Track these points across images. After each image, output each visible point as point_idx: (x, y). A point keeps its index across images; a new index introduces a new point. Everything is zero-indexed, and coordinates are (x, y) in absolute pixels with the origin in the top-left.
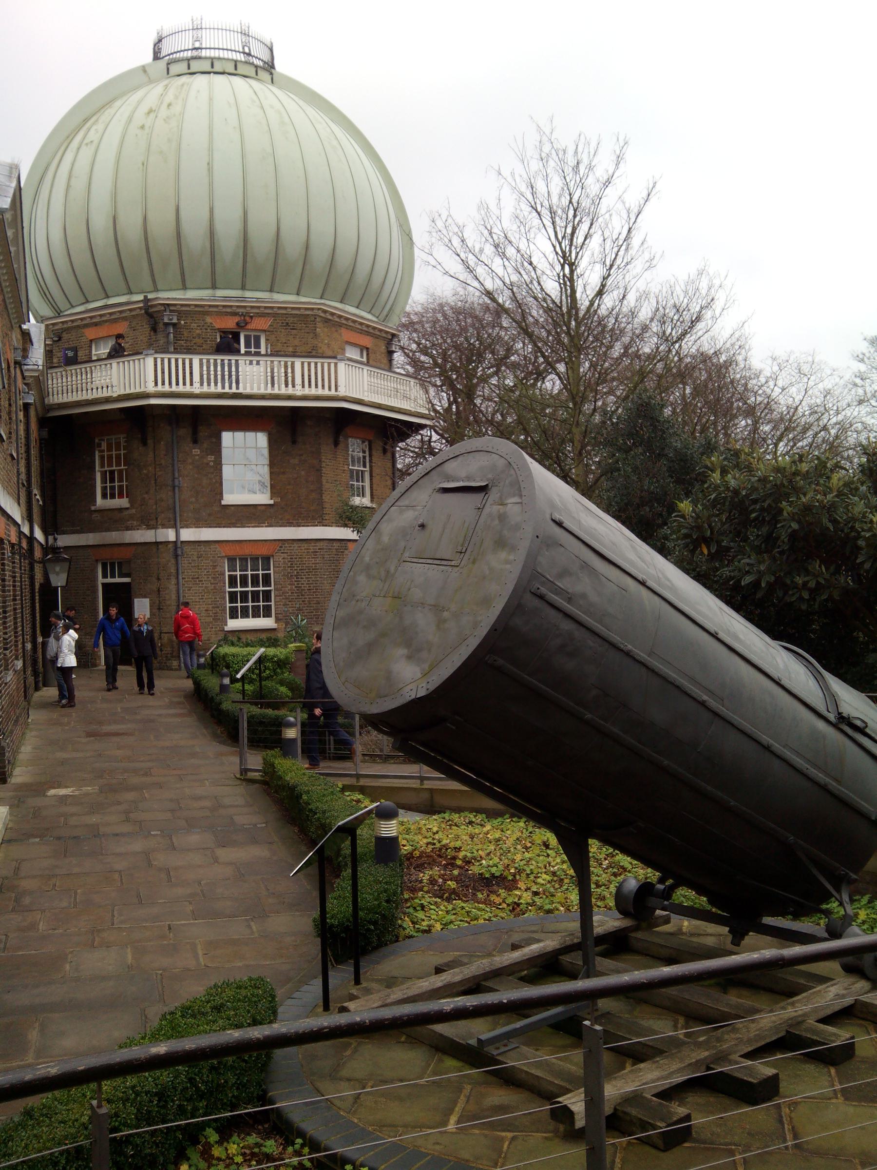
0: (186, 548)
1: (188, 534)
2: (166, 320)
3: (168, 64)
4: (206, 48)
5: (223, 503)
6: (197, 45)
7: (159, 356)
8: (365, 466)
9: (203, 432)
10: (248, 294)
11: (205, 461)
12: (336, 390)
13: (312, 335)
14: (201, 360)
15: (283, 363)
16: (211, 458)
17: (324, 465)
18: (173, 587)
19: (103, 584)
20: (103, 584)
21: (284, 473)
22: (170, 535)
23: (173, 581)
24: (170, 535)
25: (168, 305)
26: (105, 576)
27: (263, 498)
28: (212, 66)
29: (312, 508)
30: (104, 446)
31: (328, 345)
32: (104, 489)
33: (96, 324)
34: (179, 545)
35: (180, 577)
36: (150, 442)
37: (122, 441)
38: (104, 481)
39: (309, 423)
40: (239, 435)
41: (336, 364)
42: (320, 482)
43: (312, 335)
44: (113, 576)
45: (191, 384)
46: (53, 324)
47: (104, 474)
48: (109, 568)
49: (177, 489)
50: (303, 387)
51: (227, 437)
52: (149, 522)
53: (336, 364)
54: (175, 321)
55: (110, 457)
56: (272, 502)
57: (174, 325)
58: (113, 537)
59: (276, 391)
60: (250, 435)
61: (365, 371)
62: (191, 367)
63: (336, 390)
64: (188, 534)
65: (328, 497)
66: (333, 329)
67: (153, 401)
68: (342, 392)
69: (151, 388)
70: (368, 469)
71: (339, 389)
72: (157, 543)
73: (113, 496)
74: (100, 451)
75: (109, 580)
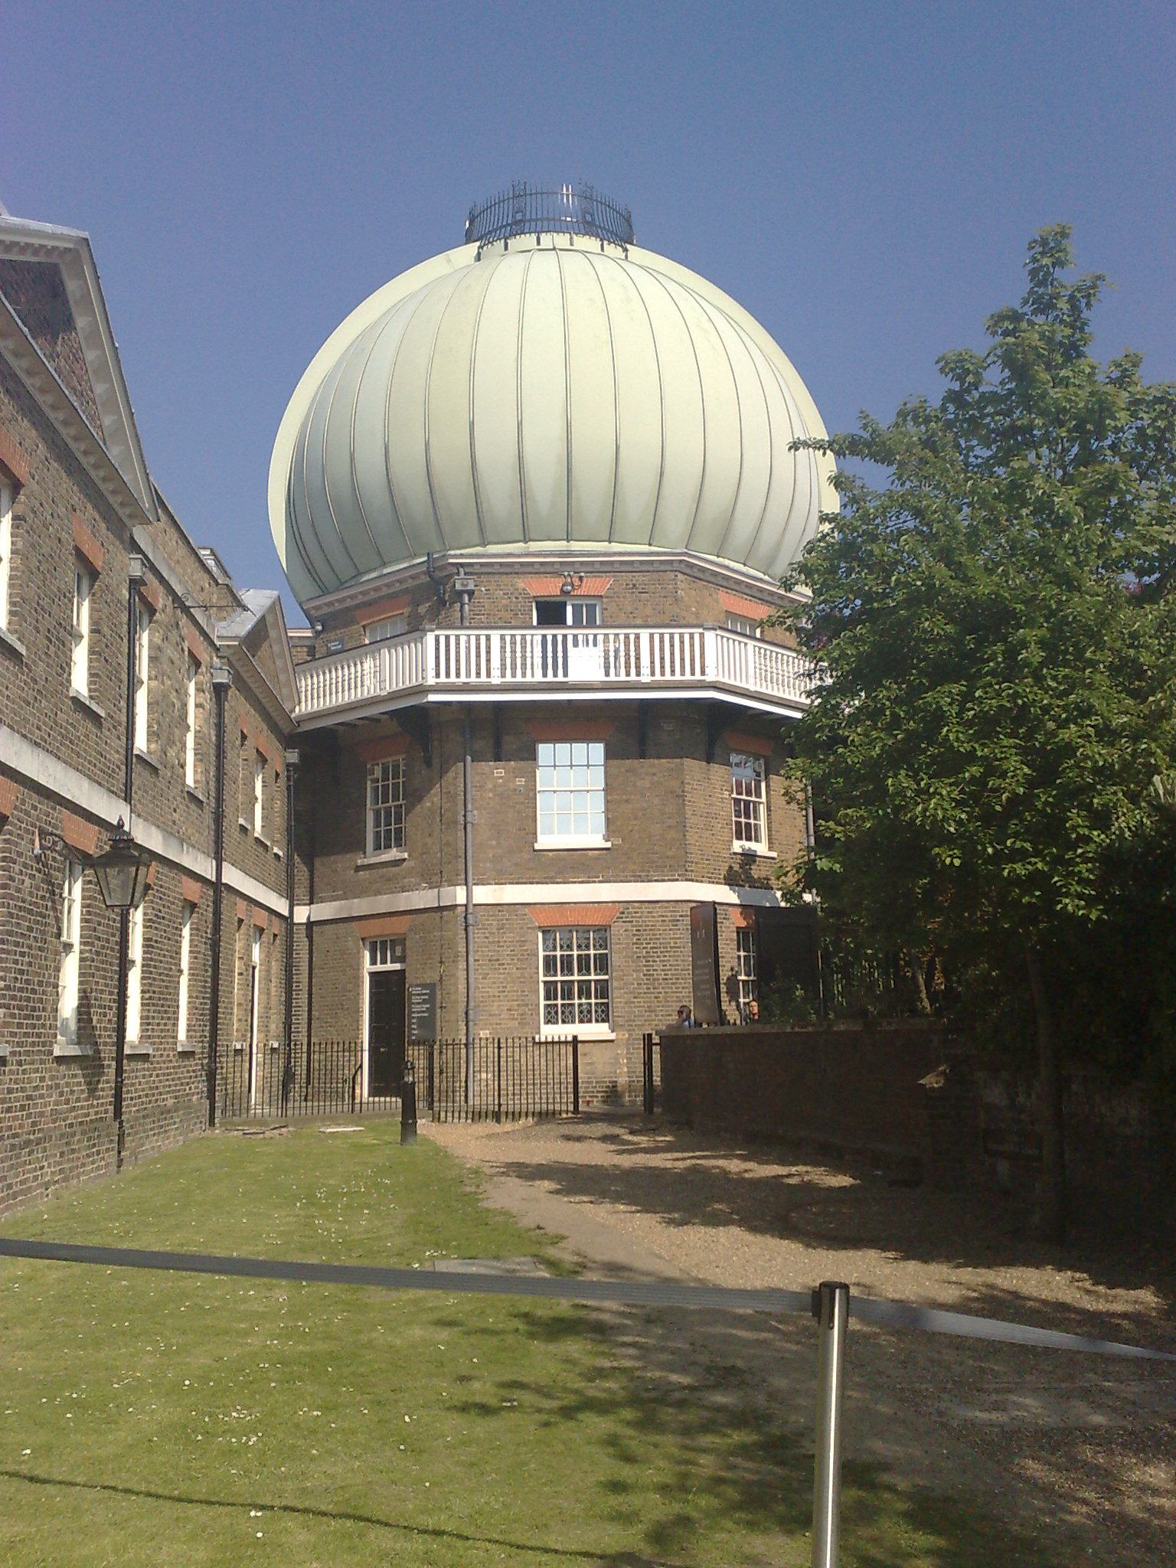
0: (481, 911)
1: (483, 894)
2: (458, 587)
3: (481, 247)
4: (530, 221)
5: (537, 846)
6: (519, 216)
7: (442, 633)
8: (758, 795)
9: (510, 742)
10: (576, 546)
11: (512, 786)
12: (703, 673)
13: (670, 600)
14: (503, 638)
15: (622, 637)
16: (521, 782)
17: (687, 788)
18: (462, 975)
19: (372, 974)
20: (372, 974)
21: (627, 801)
22: (460, 895)
23: (462, 965)
24: (460, 895)
25: (462, 565)
26: (373, 962)
27: (592, 836)
28: (538, 243)
29: (670, 853)
30: (378, 773)
31: (697, 615)
32: (377, 834)
33: (370, 604)
34: (470, 910)
35: (471, 959)
36: (436, 762)
37: (402, 763)
38: (377, 824)
39: (666, 727)
40: (563, 748)
41: (702, 635)
42: (681, 813)
43: (670, 600)
44: (384, 962)
45: (489, 675)
46: (317, 608)
47: (377, 813)
48: (379, 947)
49: (469, 826)
50: (653, 674)
51: (544, 750)
52: (436, 878)
53: (702, 635)
54: (471, 587)
55: (386, 788)
56: (608, 845)
57: (471, 593)
58: (383, 903)
59: (612, 678)
60: (580, 748)
61: (750, 647)
62: (488, 648)
63: (703, 673)
64: (483, 894)
65: (696, 837)
66: (706, 593)
67: (433, 698)
68: (711, 676)
69: (431, 681)
70: (764, 799)
71: (707, 671)
72: (440, 909)
73: (388, 847)
74: (373, 781)
75: (379, 967)
